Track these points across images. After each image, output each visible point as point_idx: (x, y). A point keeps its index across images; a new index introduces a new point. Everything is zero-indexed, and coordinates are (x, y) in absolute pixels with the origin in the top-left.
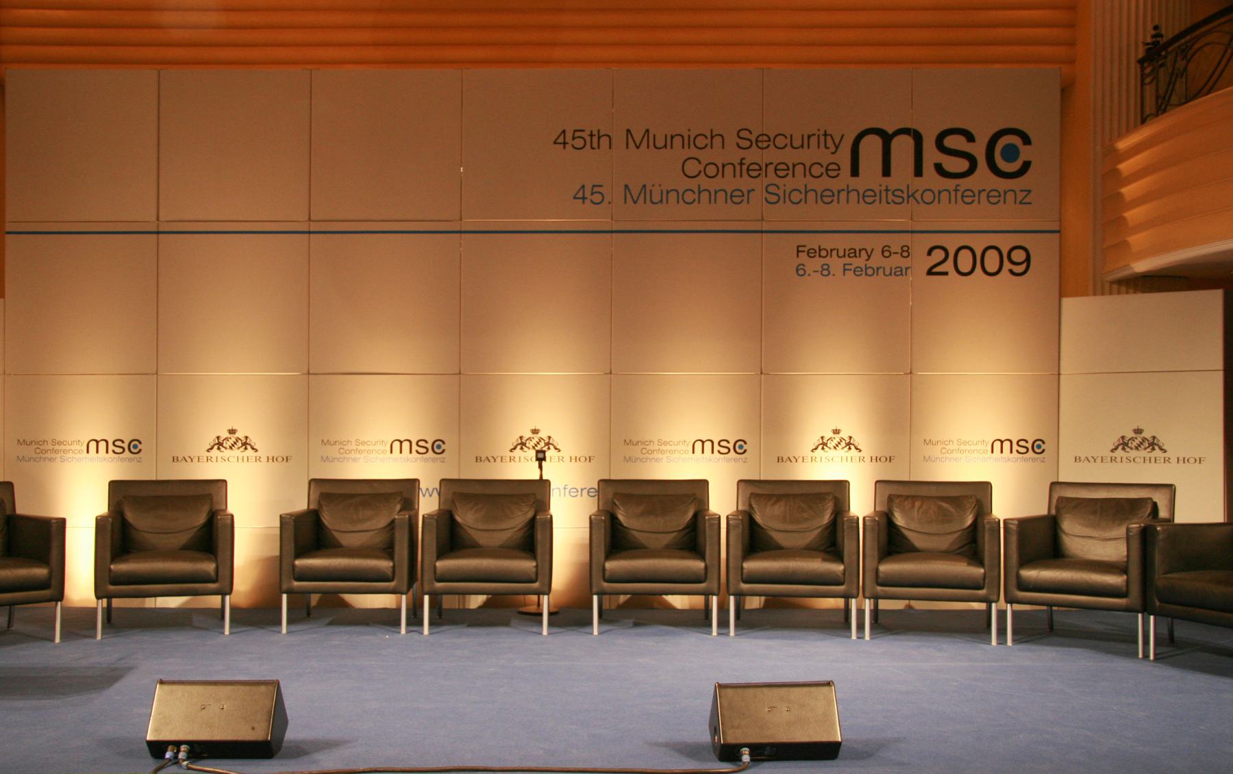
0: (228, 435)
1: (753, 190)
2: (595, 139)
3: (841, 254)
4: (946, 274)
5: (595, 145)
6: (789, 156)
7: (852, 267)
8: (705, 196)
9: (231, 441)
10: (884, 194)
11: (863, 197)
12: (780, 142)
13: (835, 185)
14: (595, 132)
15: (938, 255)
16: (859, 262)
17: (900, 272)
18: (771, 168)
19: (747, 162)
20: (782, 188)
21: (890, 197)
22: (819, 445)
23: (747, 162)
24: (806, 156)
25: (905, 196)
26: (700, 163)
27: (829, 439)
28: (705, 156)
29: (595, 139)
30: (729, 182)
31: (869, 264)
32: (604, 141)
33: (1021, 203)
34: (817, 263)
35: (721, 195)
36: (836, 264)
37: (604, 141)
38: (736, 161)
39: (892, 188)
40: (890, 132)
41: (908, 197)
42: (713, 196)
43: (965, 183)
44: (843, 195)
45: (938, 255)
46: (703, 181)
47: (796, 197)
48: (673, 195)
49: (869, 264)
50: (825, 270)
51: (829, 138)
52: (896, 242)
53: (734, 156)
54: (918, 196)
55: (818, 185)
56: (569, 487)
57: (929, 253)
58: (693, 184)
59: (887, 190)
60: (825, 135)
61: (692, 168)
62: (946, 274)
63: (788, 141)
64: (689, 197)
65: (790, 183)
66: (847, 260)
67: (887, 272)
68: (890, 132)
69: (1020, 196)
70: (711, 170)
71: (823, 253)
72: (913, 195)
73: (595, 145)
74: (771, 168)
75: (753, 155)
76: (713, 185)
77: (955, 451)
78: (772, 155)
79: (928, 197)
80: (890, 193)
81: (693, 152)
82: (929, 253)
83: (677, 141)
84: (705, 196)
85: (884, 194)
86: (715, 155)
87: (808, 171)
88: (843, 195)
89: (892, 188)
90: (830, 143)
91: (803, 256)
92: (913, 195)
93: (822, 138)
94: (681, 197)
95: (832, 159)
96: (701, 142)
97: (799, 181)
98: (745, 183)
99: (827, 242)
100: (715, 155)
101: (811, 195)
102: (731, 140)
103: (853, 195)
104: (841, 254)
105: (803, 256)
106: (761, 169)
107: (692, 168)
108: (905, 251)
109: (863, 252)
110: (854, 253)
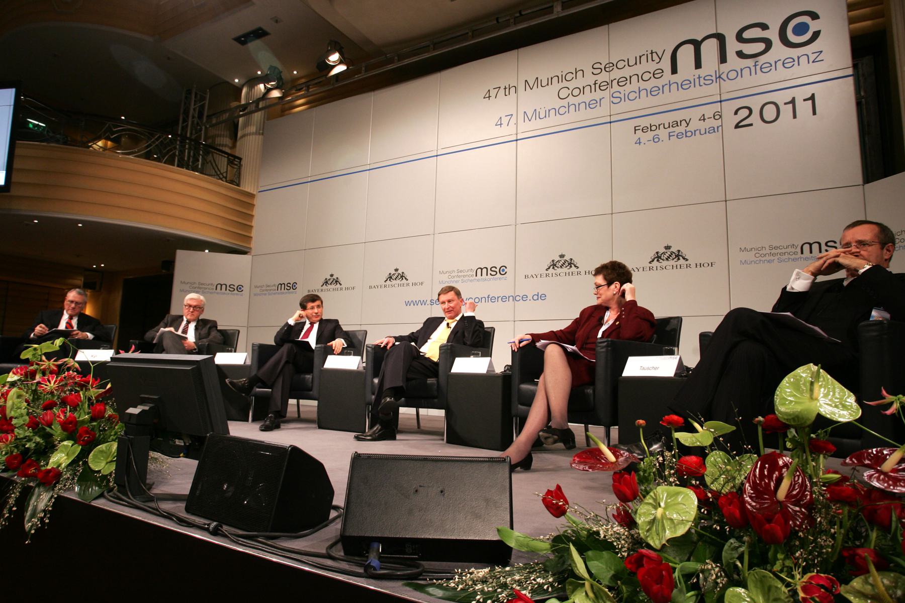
0: (330, 277)
1: (603, 98)
2: (507, 90)
3: (666, 126)
4: (751, 125)
5: (507, 93)
6: (627, 72)
7: (675, 134)
8: (572, 108)
9: (331, 281)
10: (697, 81)
11: (681, 86)
12: (620, 65)
13: (659, 83)
14: (507, 87)
15: (744, 113)
16: (681, 129)
17: (713, 130)
18: (615, 82)
19: (599, 82)
20: (623, 93)
21: (702, 81)
22: (655, 258)
23: (599, 82)
24: (639, 69)
25: (714, 78)
26: (569, 89)
27: (662, 253)
28: (571, 85)
29: (507, 90)
30: (588, 97)
31: (688, 129)
32: (513, 90)
33: (813, 62)
34: (650, 134)
35: (583, 106)
36: (663, 133)
37: (513, 90)
38: (592, 84)
39: (702, 75)
40: (700, 39)
41: (716, 79)
42: (577, 107)
43: (762, 59)
44: (667, 88)
45: (744, 113)
46: (571, 99)
47: (632, 96)
48: (553, 112)
49: (688, 129)
50: (656, 139)
51: (654, 55)
52: (709, 111)
53: (590, 79)
54: (724, 76)
55: (648, 85)
56: (491, 296)
57: (736, 113)
58: (564, 103)
59: (699, 78)
60: (652, 53)
61: (564, 93)
62: (751, 125)
63: (626, 63)
64: (562, 111)
65: (628, 88)
66: (671, 129)
67: (703, 132)
68: (700, 40)
69: (812, 58)
70: (576, 92)
71: (654, 128)
72: (720, 77)
73: (507, 93)
74: (615, 82)
75: (604, 77)
76: (576, 100)
77: (767, 255)
78: (616, 74)
79: (732, 75)
80: (702, 79)
81: (565, 84)
82: (736, 113)
83: (555, 80)
84: (572, 108)
85: (697, 81)
86: (580, 82)
87: (640, 78)
88: (667, 88)
89: (702, 75)
90: (655, 56)
91: (639, 132)
92: (720, 77)
93: (650, 56)
94: (557, 112)
95: (659, 66)
96: (569, 77)
97: (635, 85)
98: (598, 94)
99: (655, 120)
100: (580, 82)
101: (643, 93)
102: (588, 71)
103: (674, 87)
104: (666, 126)
105: (639, 132)
106: (609, 84)
107: (564, 93)
108: (718, 116)
109: (683, 122)
110: (677, 124)
